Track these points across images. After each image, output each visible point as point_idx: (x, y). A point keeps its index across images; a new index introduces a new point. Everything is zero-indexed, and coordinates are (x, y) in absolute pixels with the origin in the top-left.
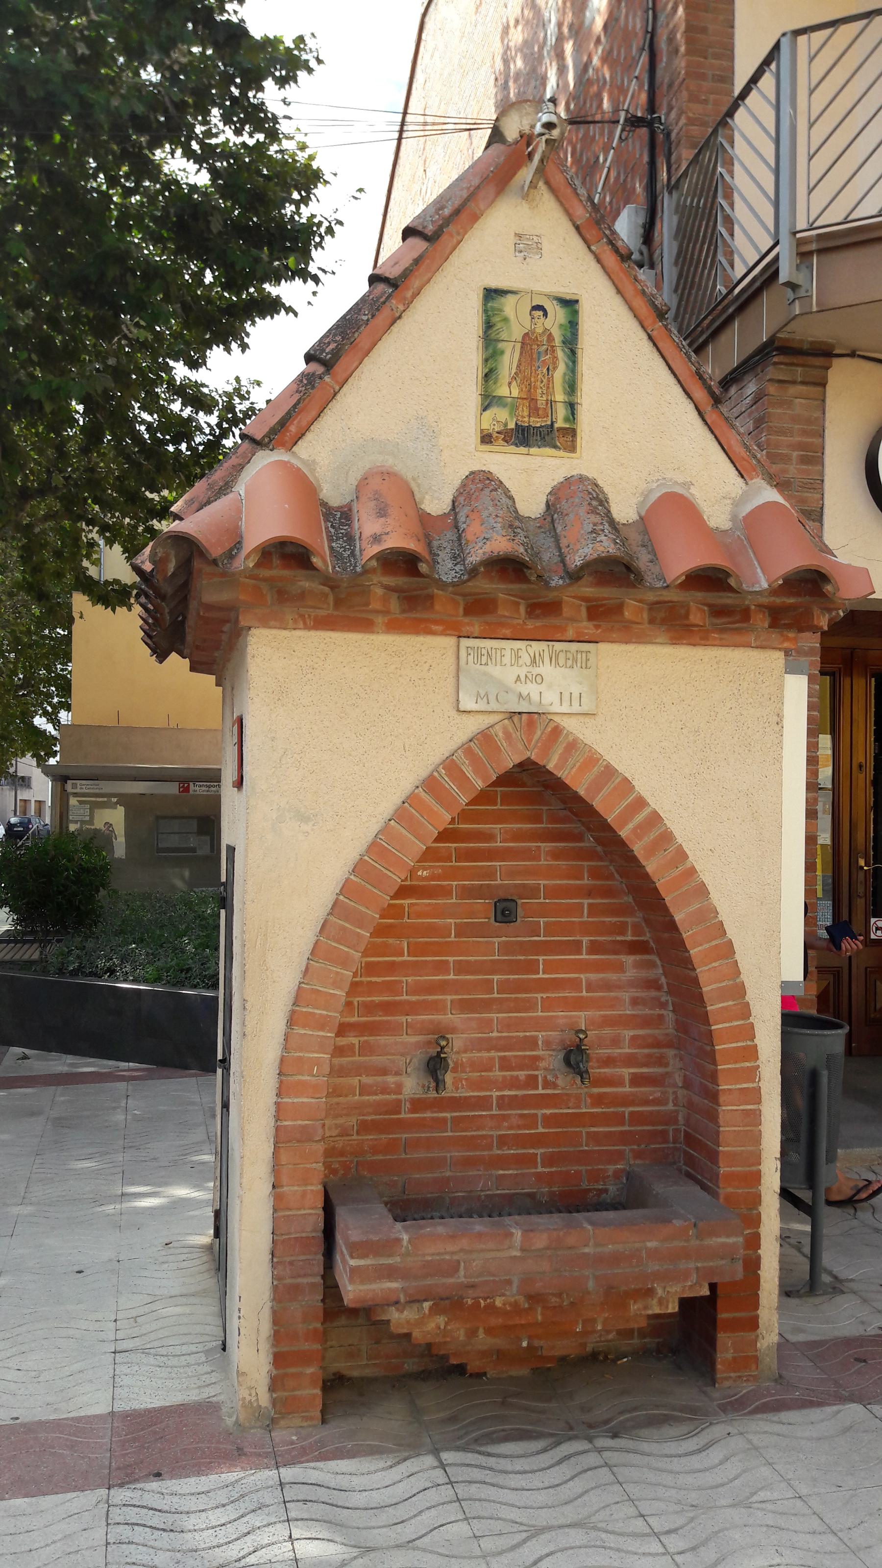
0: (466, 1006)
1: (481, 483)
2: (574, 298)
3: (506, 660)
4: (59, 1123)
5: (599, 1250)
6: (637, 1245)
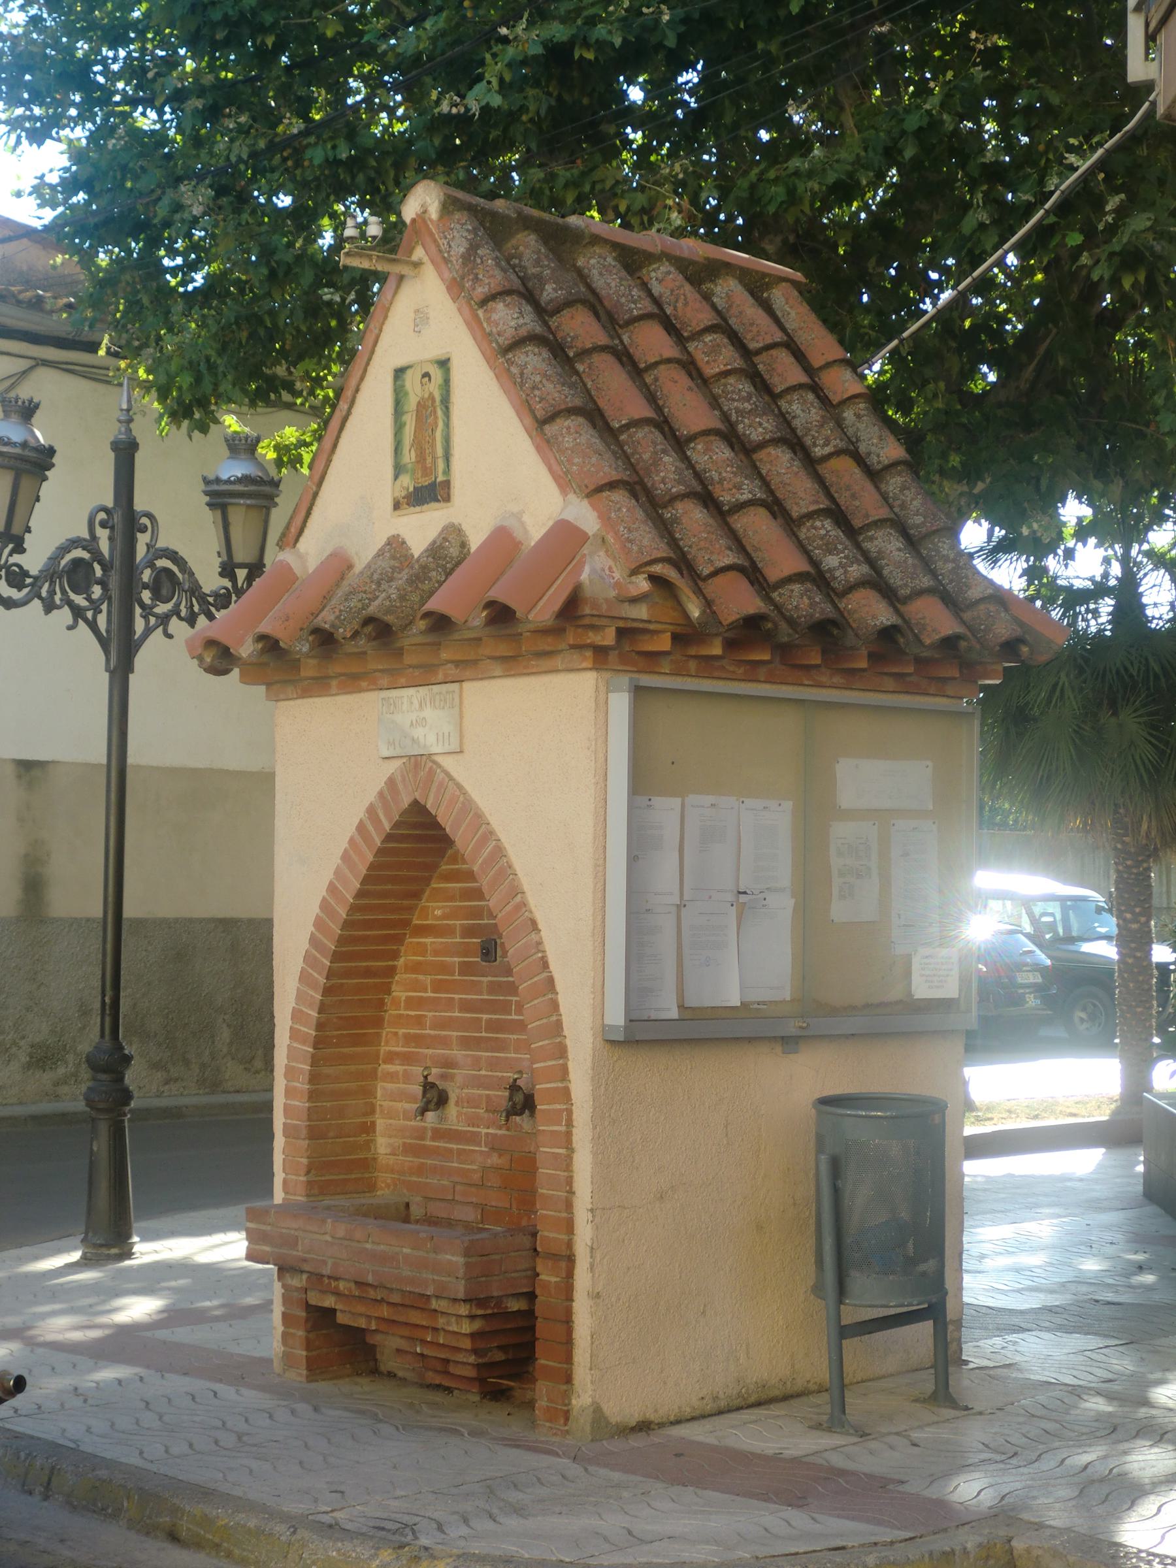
0: (466, 1043)
1: (396, 545)
2: (447, 356)
3: (405, 707)
4: (1142, 1359)
5: (375, 1247)
6: (397, 1249)
